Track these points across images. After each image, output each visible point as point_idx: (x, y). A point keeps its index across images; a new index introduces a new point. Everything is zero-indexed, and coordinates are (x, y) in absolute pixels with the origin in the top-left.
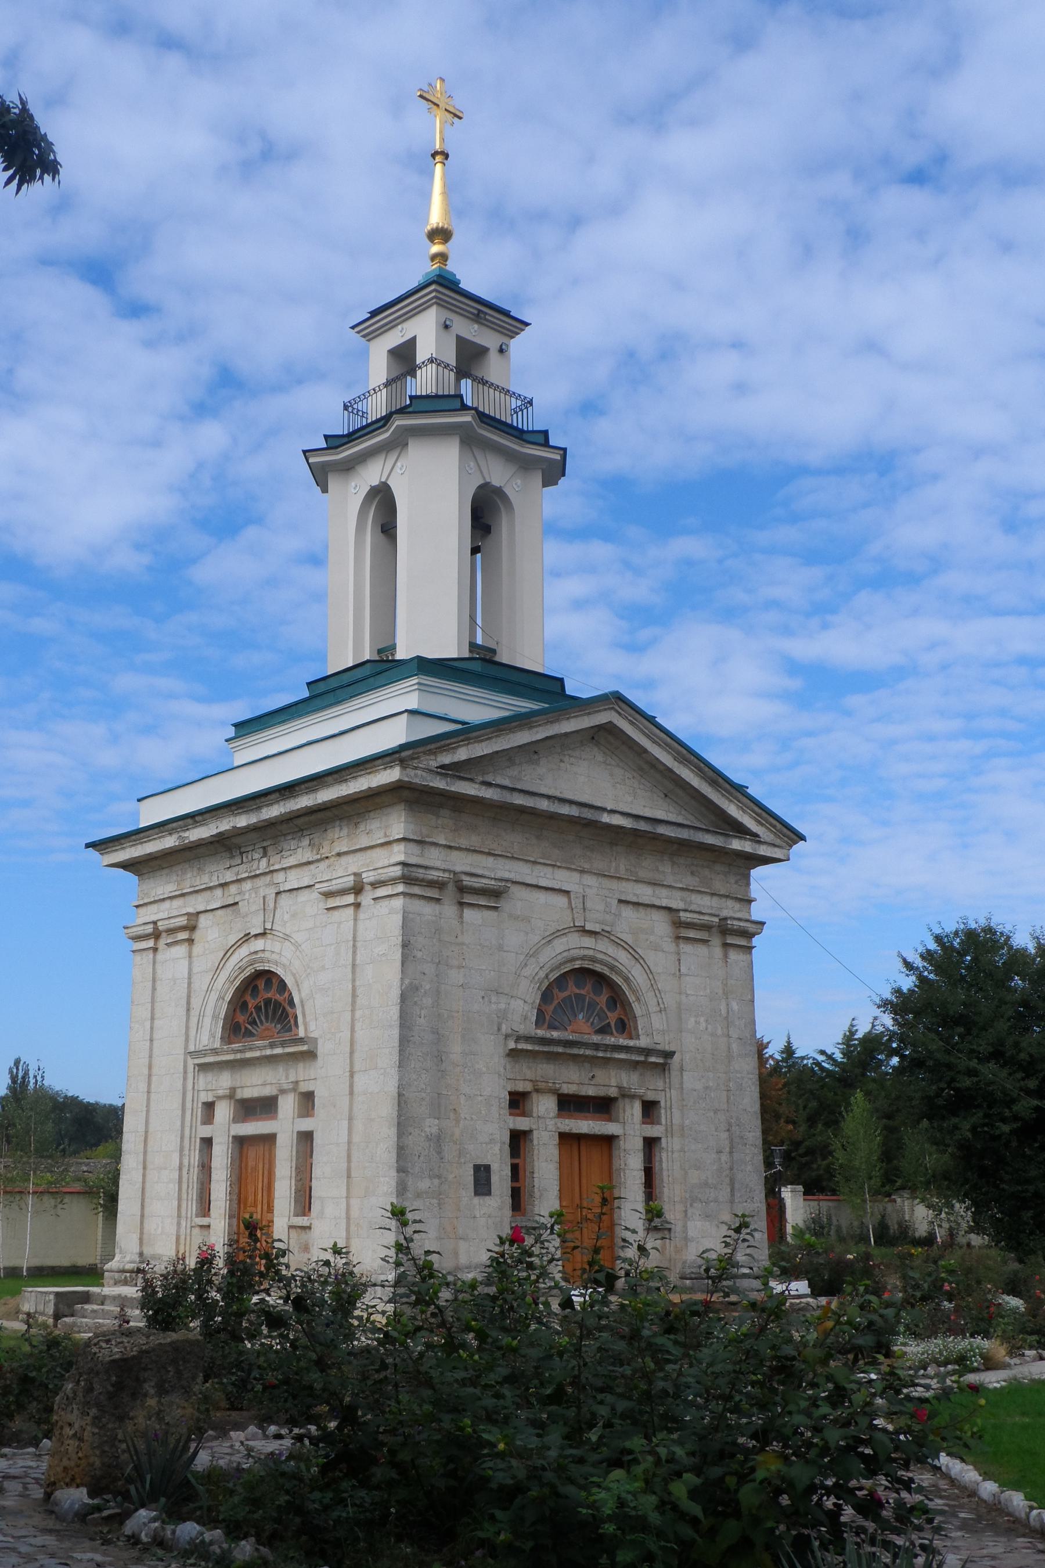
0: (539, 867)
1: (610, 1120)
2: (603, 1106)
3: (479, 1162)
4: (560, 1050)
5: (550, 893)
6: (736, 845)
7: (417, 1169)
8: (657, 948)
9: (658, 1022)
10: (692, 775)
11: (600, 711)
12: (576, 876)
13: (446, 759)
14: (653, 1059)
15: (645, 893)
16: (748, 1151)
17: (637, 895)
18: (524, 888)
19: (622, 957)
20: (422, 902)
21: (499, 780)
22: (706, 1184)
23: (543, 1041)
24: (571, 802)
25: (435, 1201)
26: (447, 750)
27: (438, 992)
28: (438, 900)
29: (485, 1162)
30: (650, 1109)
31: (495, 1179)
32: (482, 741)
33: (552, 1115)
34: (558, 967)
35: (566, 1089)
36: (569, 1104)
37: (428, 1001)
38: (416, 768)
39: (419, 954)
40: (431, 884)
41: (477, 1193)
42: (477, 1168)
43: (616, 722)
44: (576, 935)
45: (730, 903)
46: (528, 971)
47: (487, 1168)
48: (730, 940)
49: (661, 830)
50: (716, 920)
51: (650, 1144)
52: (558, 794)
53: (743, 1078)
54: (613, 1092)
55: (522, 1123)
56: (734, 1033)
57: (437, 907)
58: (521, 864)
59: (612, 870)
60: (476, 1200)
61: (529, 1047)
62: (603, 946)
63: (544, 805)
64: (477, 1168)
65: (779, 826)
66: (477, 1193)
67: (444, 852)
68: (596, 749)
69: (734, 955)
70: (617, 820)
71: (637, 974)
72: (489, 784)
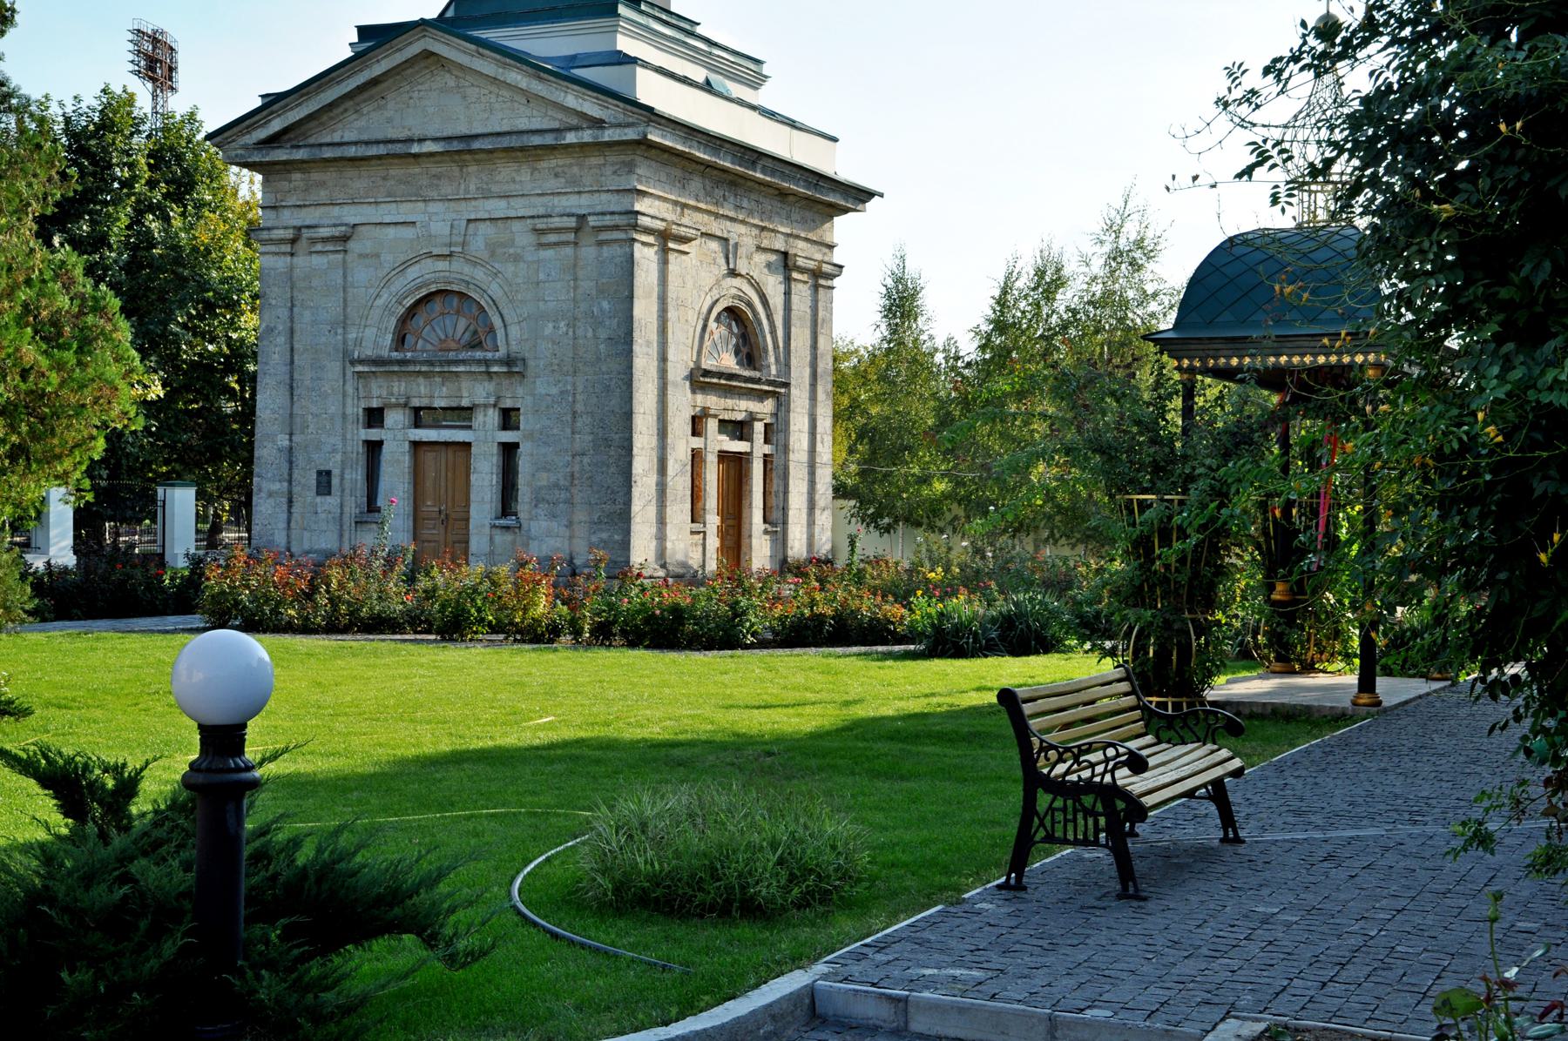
0: (383, 206)
1: (470, 427)
2: (462, 414)
3: (322, 468)
4: (396, 368)
5: (399, 227)
6: (571, 138)
7: (269, 475)
8: (517, 259)
9: (514, 331)
10: (519, 77)
11: (411, 43)
12: (421, 205)
13: (262, 134)
14: (495, 369)
15: (498, 207)
16: (612, 453)
17: (489, 212)
18: (373, 227)
19: (479, 274)
20: (276, 258)
21: (328, 139)
22: (556, 486)
23: (390, 362)
24: (378, 142)
25: (284, 500)
26: (261, 126)
27: (292, 331)
28: (292, 255)
29: (327, 468)
30: (508, 418)
31: (335, 481)
32: (292, 109)
33: (400, 426)
34: (411, 292)
35: (416, 403)
36: (419, 416)
37: (281, 340)
38: (235, 149)
39: (274, 302)
40: (281, 241)
41: (318, 494)
42: (319, 473)
43: (431, 48)
44: (429, 261)
45: (604, 197)
46: (380, 302)
47: (329, 473)
48: (604, 236)
49: (476, 145)
50: (574, 219)
51: (509, 450)
52: (365, 137)
53: (611, 379)
54: (465, 403)
55: (374, 434)
56: (603, 334)
57: (289, 258)
58: (365, 206)
59: (461, 191)
60: (319, 499)
61: (366, 369)
62: (457, 265)
63: (352, 151)
64: (319, 473)
65: (621, 105)
66: (318, 494)
67: (296, 211)
68: (448, 75)
69: (606, 251)
70: (429, 147)
71: (495, 289)
72: (299, 147)
